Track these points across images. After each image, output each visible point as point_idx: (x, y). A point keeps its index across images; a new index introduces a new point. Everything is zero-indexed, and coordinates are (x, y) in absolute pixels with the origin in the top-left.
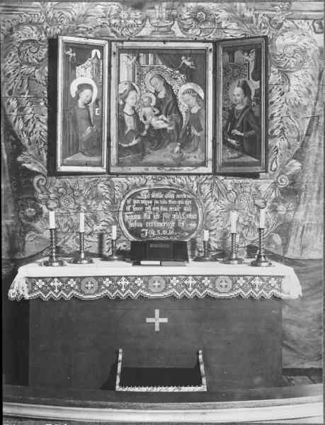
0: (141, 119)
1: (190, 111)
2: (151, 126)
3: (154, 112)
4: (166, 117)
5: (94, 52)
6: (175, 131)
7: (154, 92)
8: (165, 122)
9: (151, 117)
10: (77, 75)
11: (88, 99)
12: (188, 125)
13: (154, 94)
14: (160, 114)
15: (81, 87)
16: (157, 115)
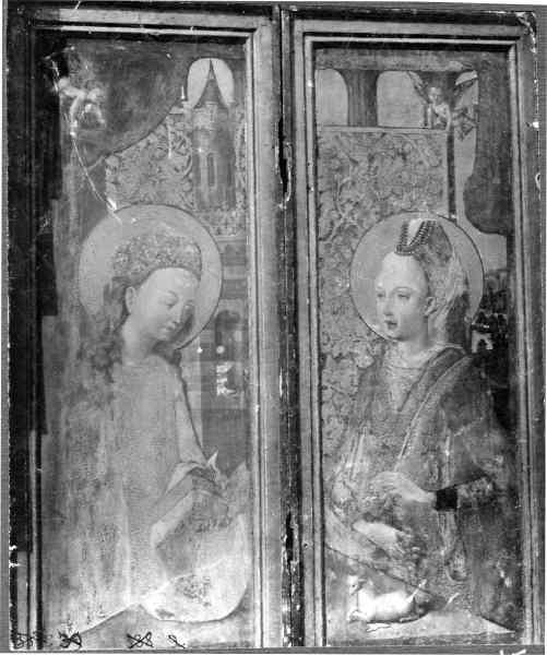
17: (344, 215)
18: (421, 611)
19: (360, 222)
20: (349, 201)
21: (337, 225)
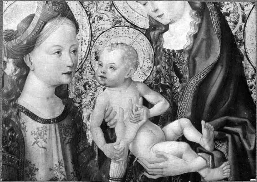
0: (95, 136)
3: (147, 104)
7: (144, 24)
8: (195, 147)
9: (132, 128)
13: (147, 33)
14: (172, 115)
16: (160, 121)
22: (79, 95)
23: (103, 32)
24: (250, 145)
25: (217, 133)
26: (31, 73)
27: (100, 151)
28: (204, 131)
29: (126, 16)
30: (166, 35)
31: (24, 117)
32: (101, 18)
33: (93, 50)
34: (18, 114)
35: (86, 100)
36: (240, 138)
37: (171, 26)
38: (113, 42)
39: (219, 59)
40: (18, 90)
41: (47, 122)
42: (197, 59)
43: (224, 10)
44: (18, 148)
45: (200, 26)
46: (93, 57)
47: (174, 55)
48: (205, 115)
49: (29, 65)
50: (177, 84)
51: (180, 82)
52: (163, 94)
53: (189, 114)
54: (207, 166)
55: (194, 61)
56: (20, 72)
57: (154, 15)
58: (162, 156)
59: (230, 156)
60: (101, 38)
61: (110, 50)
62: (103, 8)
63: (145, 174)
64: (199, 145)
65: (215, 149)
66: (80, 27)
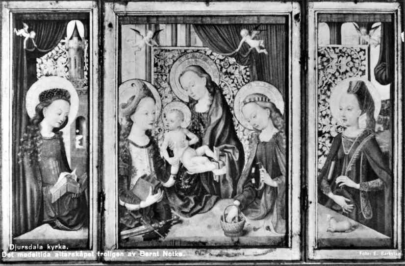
0: (164, 154)
1: (258, 137)
2: (182, 169)
3: (188, 139)
4: (212, 149)
5: (70, 26)
6: (228, 178)
7: (187, 100)
8: (210, 159)
10: (39, 75)
11: (62, 118)
12: (254, 164)
13: (188, 104)
15: (47, 97)
17: (328, 79)
18: (353, 228)
19: (334, 81)
20: (330, 73)
21: (325, 83)
22: (157, 134)
23: (168, 104)
24: (236, 158)
25: (221, 152)
26: (134, 124)
27: (166, 161)
28: (215, 151)
29: (178, 96)
30: (197, 106)
31: (131, 145)
32: (166, 97)
33: (163, 113)
34: (128, 144)
35: (160, 137)
36: (231, 155)
37: (199, 101)
38: (173, 109)
39: (222, 117)
40: (128, 132)
41: (142, 147)
42: (212, 117)
43: (224, 93)
44: (128, 160)
45: (213, 101)
46: (163, 115)
47: (201, 115)
48: (215, 144)
49: (133, 120)
50: (202, 129)
51: (204, 128)
52: (196, 134)
53: (208, 143)
54: (216, 168)
55: (210, 118)
56: (129, 124)
57: (191, 96)
58: (194, 164)
59: (227, 163)
60: (166, 107)
61: (170, 113)
62: (168, 92)
63: (187, 172)
64: (212, 158)
65: (220, 160)
66: (157, 102)
